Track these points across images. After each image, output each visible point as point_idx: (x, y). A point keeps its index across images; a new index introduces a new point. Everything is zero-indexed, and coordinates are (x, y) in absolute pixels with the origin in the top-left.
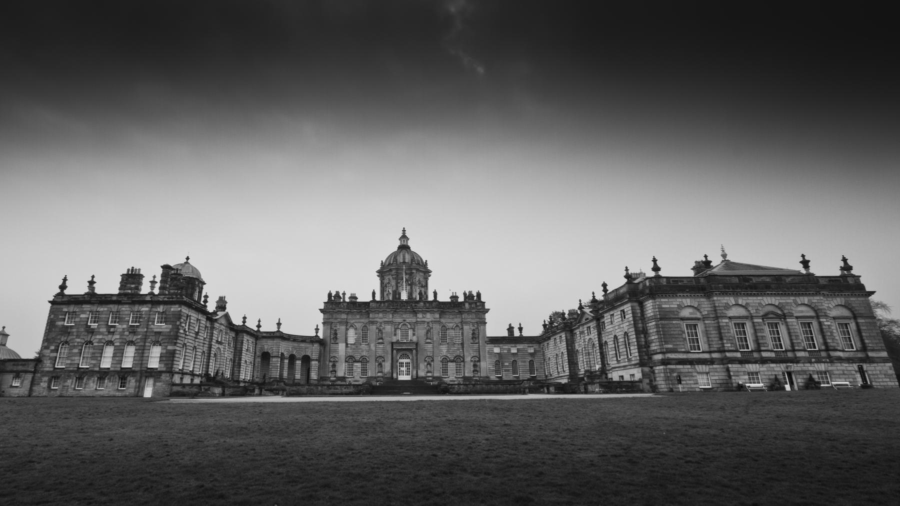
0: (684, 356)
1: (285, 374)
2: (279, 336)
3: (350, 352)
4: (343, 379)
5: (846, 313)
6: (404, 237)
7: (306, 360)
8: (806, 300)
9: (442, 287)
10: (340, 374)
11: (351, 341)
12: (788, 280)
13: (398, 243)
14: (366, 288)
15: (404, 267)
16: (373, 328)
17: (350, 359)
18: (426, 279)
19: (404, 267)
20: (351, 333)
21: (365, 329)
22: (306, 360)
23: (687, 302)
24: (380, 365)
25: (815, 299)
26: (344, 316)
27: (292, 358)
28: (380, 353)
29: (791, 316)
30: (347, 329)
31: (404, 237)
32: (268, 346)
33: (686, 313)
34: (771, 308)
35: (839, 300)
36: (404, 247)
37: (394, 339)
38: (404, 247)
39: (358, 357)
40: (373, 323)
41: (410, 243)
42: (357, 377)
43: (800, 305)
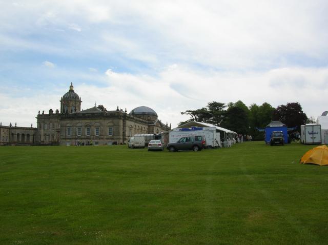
0: (64, 137)
1: (20, 140)
2: (16, 128)
3: (45, 133)
4: (43, 141)
5: (111, 124)
6: (71, 86)
7: (28, 135)
8: (98, 121)
9: (85, 106)
10: (42, 140)
11: (46, 128)
12: (87, 115)
13: (69, 89)
14: (57, 107)
15: (71, 99)
16: (51, 124)
17: (45, 135)
18: (80, 104)
19: (71, 99)
20: (46, 125)
21: (49, 124)
22: (28, 135)
23: (68, 122)
24: (53, 137)
25: (101, 120)
26: (43, 120)
27: (23, 135)
28: (53, 133)
29: (93, 126)
30: (44, 124)
31: (71, 86)
32: (13, 131)
33: (68, 125)
34: (88, 124)
35: (110, 121)
36: (71, 91)
37: (58, 128)
38: (71, 91)
39: (47, 134)
40: (51, 122)
41: (74, 89)
42: (47, 142)
43: (96, 122)
